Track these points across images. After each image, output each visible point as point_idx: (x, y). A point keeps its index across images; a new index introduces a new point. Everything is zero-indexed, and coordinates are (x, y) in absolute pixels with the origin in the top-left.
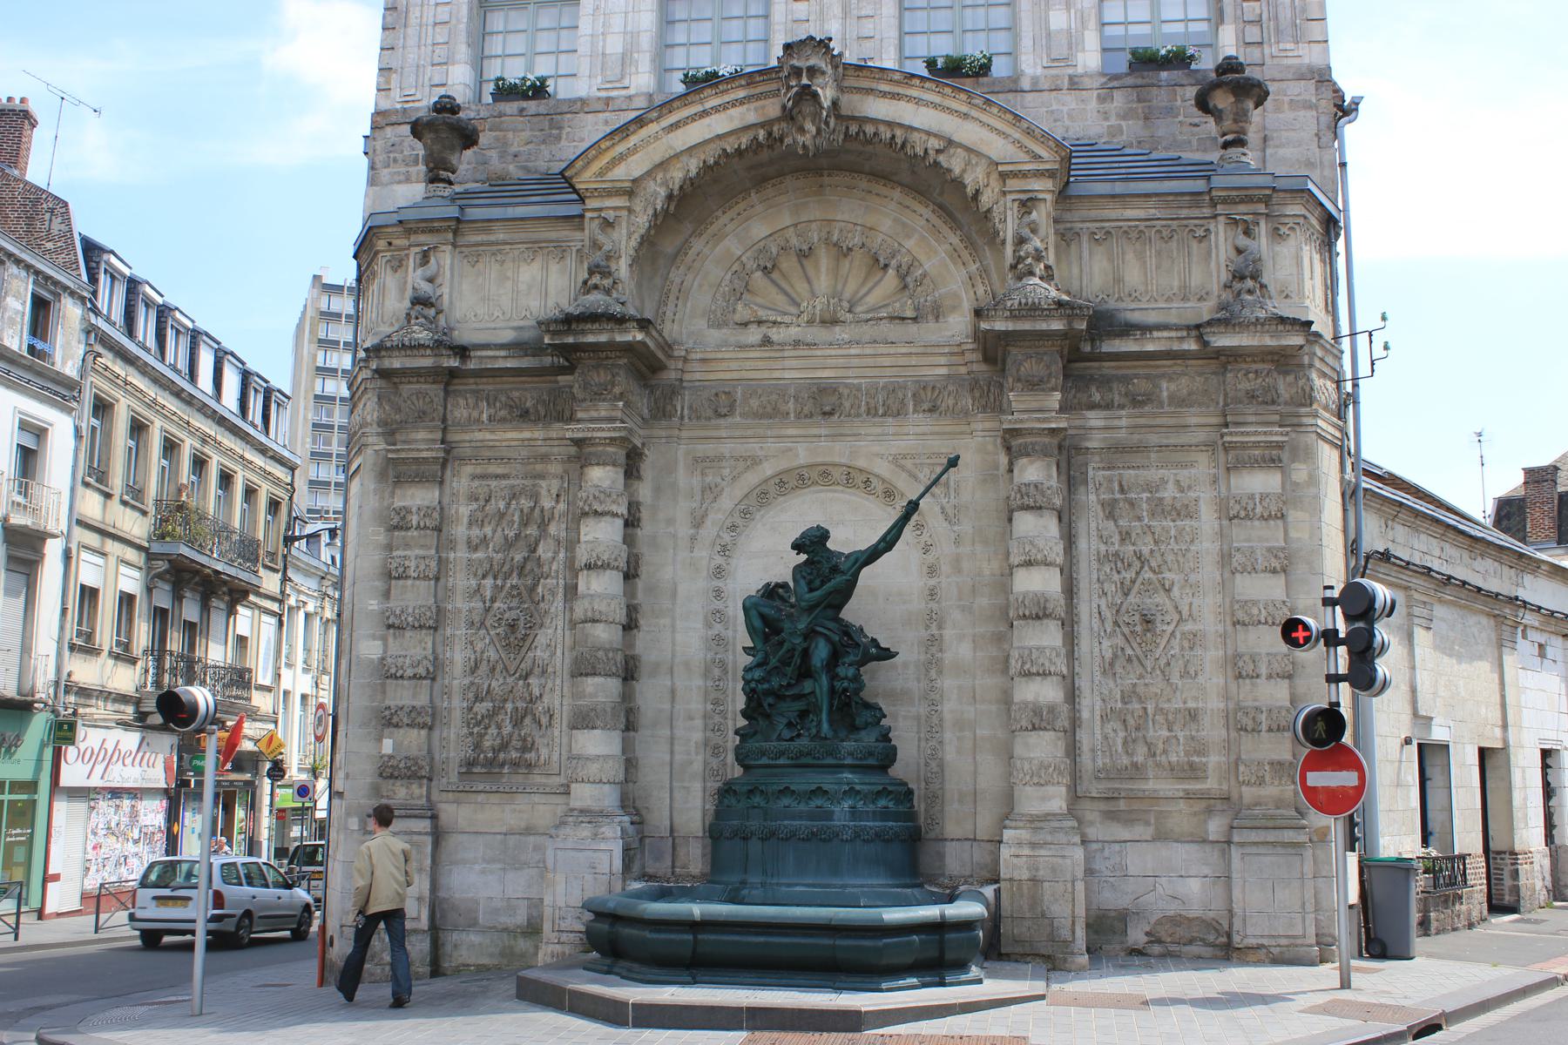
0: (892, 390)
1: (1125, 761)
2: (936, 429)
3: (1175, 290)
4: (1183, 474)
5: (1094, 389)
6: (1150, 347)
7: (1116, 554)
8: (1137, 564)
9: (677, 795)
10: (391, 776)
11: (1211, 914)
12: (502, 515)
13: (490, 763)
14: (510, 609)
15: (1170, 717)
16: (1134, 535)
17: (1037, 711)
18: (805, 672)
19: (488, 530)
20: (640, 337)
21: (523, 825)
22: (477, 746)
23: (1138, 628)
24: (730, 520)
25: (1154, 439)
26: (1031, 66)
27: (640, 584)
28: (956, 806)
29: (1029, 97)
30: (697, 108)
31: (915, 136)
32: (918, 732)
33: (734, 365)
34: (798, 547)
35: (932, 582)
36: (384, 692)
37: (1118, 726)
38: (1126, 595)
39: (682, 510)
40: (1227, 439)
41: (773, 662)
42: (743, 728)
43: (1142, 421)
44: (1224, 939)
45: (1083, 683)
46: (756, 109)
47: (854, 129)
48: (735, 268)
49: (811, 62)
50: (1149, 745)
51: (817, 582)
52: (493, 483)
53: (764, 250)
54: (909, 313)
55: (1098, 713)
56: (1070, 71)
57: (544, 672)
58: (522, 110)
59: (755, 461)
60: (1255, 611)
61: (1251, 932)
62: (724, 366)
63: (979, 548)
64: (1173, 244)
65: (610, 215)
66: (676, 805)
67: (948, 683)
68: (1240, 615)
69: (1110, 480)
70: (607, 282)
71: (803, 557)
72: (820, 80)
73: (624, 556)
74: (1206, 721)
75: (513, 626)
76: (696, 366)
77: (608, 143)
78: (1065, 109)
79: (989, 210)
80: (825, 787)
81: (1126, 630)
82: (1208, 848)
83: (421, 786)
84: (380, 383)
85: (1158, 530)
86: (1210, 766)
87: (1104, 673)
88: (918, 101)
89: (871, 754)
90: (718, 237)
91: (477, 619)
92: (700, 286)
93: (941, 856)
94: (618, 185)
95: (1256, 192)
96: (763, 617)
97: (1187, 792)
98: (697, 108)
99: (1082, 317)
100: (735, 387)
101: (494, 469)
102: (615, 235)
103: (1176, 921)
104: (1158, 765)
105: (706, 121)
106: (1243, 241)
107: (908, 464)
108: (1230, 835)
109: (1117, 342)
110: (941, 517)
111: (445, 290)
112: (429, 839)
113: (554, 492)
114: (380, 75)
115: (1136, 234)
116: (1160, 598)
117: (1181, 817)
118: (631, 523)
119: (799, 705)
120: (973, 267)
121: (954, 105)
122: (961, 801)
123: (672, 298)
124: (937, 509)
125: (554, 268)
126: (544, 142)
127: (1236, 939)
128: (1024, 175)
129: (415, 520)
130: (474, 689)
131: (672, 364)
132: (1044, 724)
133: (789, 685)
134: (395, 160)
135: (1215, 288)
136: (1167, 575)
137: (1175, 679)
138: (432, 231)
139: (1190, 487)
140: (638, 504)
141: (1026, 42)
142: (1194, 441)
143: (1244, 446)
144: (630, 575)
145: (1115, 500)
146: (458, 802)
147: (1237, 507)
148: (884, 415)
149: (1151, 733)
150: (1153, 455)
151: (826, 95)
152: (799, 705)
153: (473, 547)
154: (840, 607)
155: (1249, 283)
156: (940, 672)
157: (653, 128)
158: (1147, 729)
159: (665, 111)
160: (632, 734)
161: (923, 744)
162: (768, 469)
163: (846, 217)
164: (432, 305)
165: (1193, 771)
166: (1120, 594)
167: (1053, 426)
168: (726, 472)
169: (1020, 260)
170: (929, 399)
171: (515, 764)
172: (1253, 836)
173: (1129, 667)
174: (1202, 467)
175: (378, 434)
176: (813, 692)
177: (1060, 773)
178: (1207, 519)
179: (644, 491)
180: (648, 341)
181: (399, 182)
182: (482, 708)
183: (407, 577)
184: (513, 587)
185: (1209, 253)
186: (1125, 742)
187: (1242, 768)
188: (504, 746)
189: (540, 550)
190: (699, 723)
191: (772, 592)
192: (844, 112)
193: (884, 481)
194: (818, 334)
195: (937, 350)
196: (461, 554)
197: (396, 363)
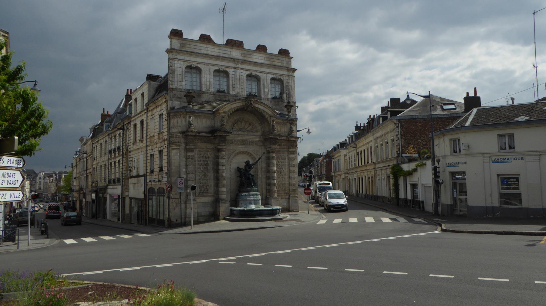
22: (201, 190)
26: (262, 96)
34: (245, 163)
61: (291, 210)
153: (198, 161)
182: (201, 185)
196: (197, 162)
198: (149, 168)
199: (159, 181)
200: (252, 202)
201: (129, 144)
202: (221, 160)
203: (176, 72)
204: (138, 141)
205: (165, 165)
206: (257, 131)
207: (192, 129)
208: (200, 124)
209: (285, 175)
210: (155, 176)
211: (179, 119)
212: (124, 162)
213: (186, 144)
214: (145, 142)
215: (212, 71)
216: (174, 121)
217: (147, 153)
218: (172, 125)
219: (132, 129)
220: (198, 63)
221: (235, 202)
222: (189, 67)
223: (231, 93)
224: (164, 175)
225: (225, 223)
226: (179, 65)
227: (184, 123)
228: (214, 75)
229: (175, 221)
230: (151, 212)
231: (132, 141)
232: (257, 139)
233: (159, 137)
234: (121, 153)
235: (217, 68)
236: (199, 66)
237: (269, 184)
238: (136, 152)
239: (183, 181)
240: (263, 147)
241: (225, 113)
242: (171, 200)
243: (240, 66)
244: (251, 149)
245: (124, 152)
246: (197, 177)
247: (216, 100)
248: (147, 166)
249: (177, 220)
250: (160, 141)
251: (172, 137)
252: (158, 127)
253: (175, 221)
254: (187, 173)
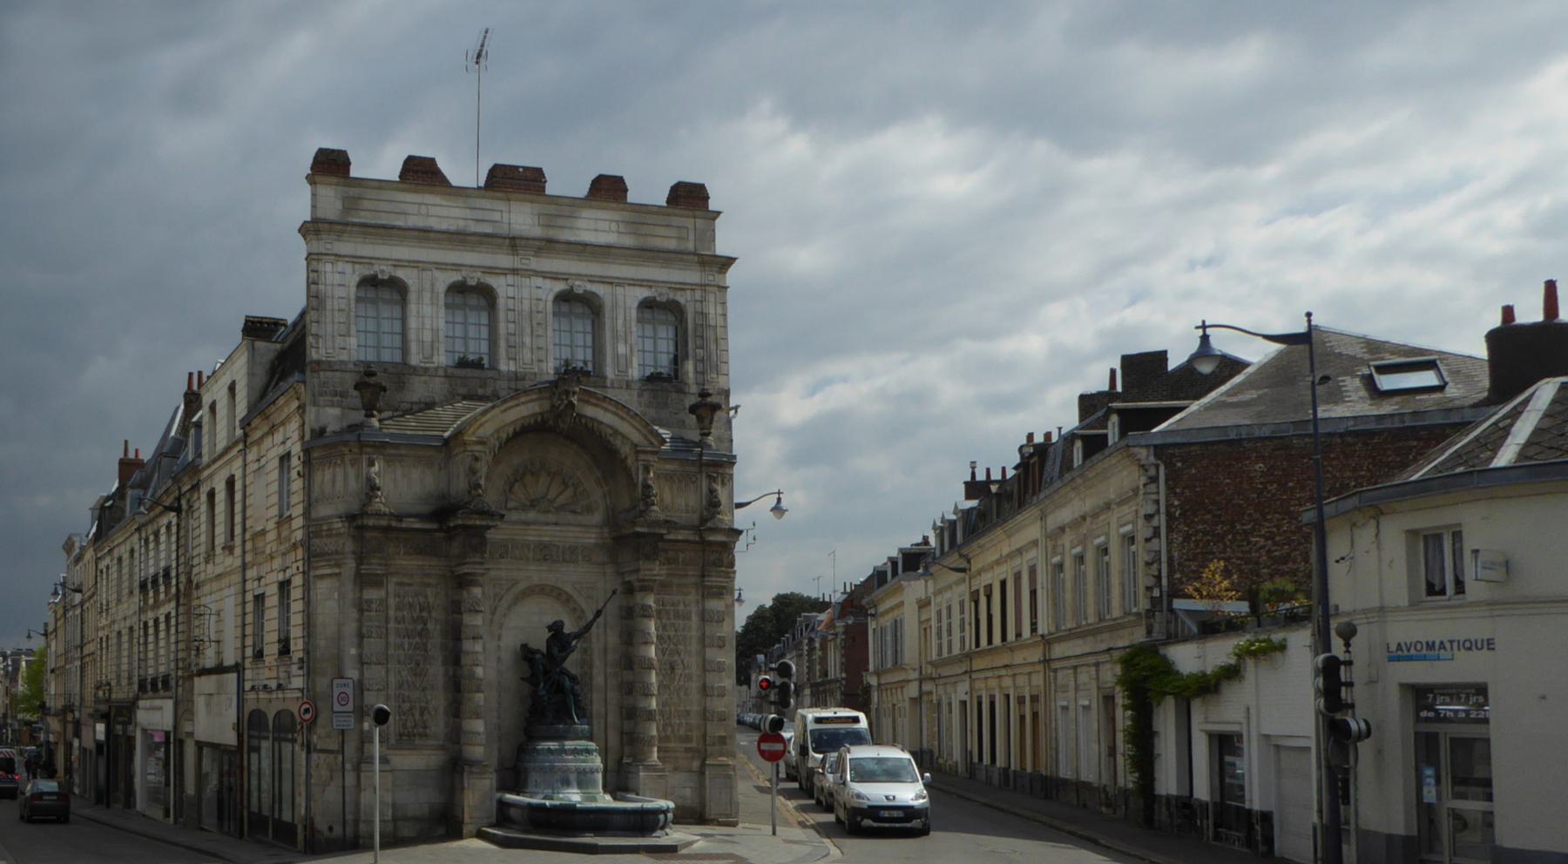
12: (411, 605)
101: (406, 580)
196: (392, 625)
198: (249, 641)
199: (280, 687)
200: (573, 777)
201: (196, 561)
202: (468, 619)
204: (218, 550)
205: (296, 632)
206: (589, 510)
207: (379, 504)
208: (402, 486)
209: (689, 678)
210: (267, 674)
211: (339, 471)
212: (181, 619)
213: (360, 559)
214: (238, 551)
215: (441, 288)
216: (324, 477)
217: (244, 592)
218: (316, 493)
219: (204, 508)
221: (514, 776)
222: (370, 282)
223: (503, 366)
224: (294, 669)
225: (482, 851)
227: (353, 484)
228: (447, 306)
229: (326, 833)
230: (255, 794)
231: (203, 549)
232: (590, 538)
233: (279, 535)
234: (173, 590)
235: (455, 277)
237: (631, 714)
238: (215, 585)
239: (350, 691)
240: (610, 569)
241: (481, 442)
242: (314, 756)
244: (570, 576)
245: (182, 587)
246: (392, 679)
247: (451, 398)
248: (244, 636)
249: (331, 829)
250: (283, 548)
251: (318, 534)
252: (275, 499)
253: (326, 833)
254: (362, 662)
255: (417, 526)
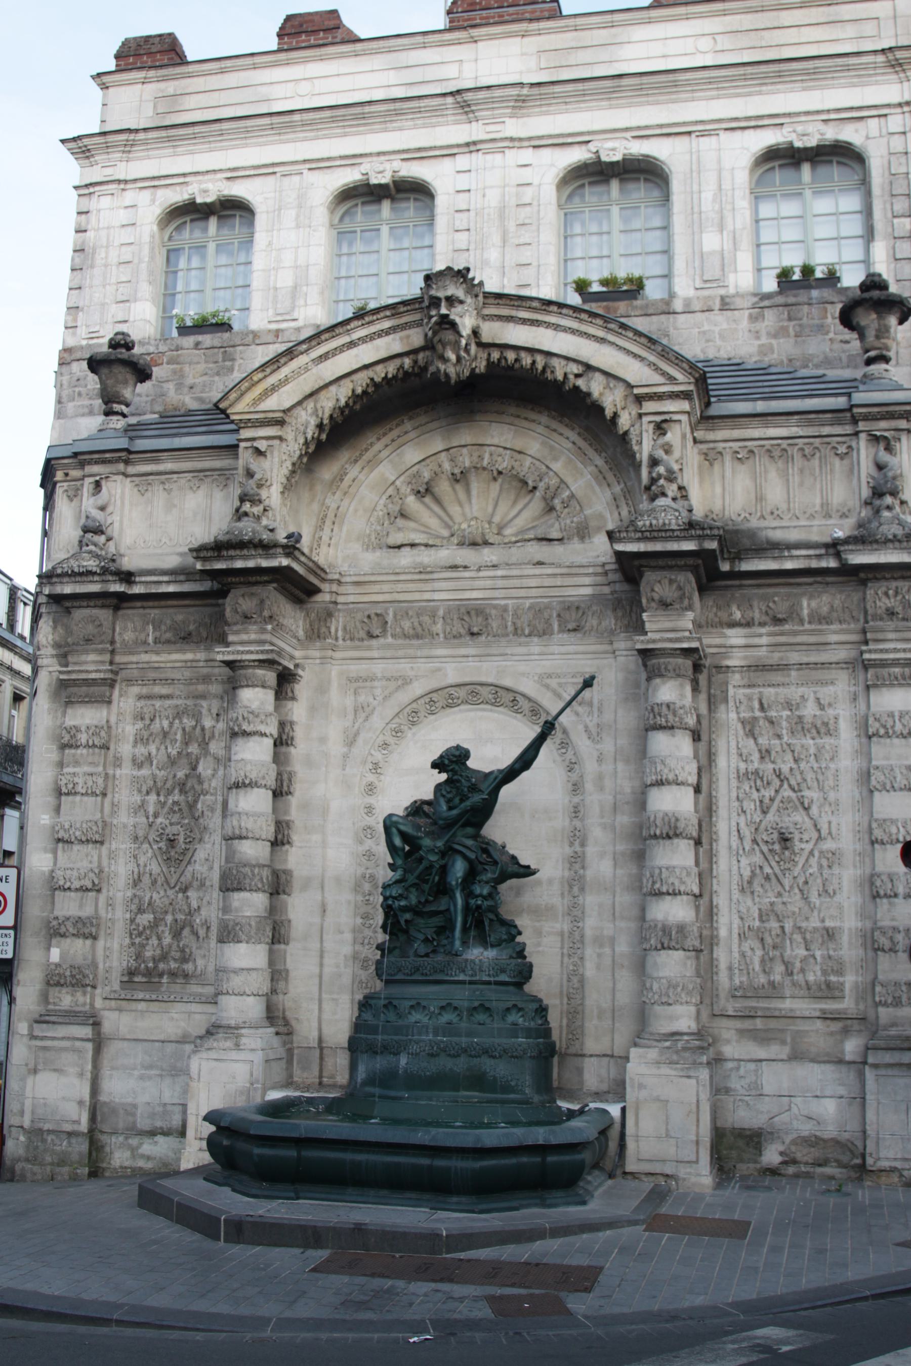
0: (538, 611)
1: (763, 979)
2: (581, 648)
3: (818, 508)
4: (826, 693)
5: (734, 608)
6: (789, 565)
7: (756, 773)
8: (777, 782)
9: (325, 1006)
10: (58, 984)
11: (846, 1136)
12: (165, 734)
13: (148, 973)
14: (171, 824)
15: (808, 936)
16: (773, 754)
17: (666, 930)
18: (443, 890)
19: (153, 748)
20: (285, 562)
21: (180, 1032)
22: (138, 956)
23: (777, 847)
24: (381, 738)
25: (795, 657)
26: (684, 288)
27: (294, 801)
28: (595, 1022)
29: (682, 318)
30: (345, 339)
31: (555, 362)
32: (562, 948)
33: (386, 587)
35: (576, 800)
36: (53, 903)
37: (756, 944)
38: (764, 812)
39: (334, 730)
40: (866, 656)
41: (411, 879)
42: (384, 943)
43: (782, 639)
44: (858, 1161)
45: (721, 901)
46: (401, 339)
47: (495, 355)
48: (390, 491)
49: (449, 293)
50: (786, 964)
51: (457, 800)
52: (158, 704)
53: (418, 475)
54: (555, 535)
55: (735, 931)
56: (722, 292)
57: (202, 885)
58: (197, 345)
59: (406, 681)
60: (894, 830)
62: (376, 588)
63: (620, 766)
64: (816, 462)
65: (262, 445)
66: (325, 1016)
67: (590, 900)
68: (878, 833)
69: (750, 699)
70: (257, 510)
71: (444, 777)
72: (459, 309)
73: (273, 775)
74: (845, 939)
75: (172, 842)
76: (350, 589)
77: (260, 375)
78: (717, 329)
79: (626, 433)
80: (455, 1003)
81: (765, 848)
82: (844, 1068)
83: (84, 994)
84: (54, 608)
85: (798, 749)
86: (848, 986)
87: (742, 890)
88: (557, 327)
89: (503, 971)
90: (373, 463)
91: (141, 833)
92: (356, 511)
93: (580, 1071)
94: (271, 415)
95: (897, 408)
96: (404, 836)
97: (823, 1011)
98: (345, 339)
99: (712, 537)
100: (387, 609)
101: (158, 690)
102: (266, 464)
103: (813, 1141)
104: (794, 984)
105: (354, 351)
106: (884, 456)
107: (553, 683)
108: (866, 1056)
109: (756, 561)
110: (584, 736)
111: (116, 518)
112: (89, 1046)
113: (214, 711)
114: (67, 314)
115: (778, 452)
116: (798, 816)
117: (818, 1035)
118: (282, 741)
119: (437, 921)
120: (617, 489)
121: (592, 330)
122: (600, 1017)
123: (328, 523)
124: (581, 727)
125: (218, 495)
126: (218, 374)
127: (870, 1161)
128: (659, 397)
129: (83, 738)
130: (136, 901)
131: (325, 587)
132: (673, 944)
133: (427, 901)
134: (80, 394)
135: (854, 503)
136: (806, 793)
137: (814, 899)
138: (104, 462)
139: (830, 705)
140: (292, 723)
141: (679, 265)
142: (834, 659)
143: (883, 664)
144: (279, 793)
145: (755, 719)
146: (120, 1010)
147: (877, 725)
148: (530, 635)
149: (789, 951)
150: (793, 673)
151: (466, 322)
152: (437, 921)
153: (137, 764)
154: (480, 825)
155: (888, 500)
156: (582, 889)
157: (302, 360)
158: (783, 948)
159: (314, 343)
160: (282, 946)
161: (566, 959)
162: (418, 688)
163: (496, 441)
164: (102, 533)
165: (830, 991)
166: (759, 812)
167: (685, 645)
168: (378, 692)
169: (653, 481)
170: (572, 619)
171: (173, 974)
172: (889, 1058)
173: (767, 886)
174: (841, 686)
175: (53, 656)
176: (448, 910)
177: (689, 993)
178: (846, 736)
179: (298, 711)
180: (296, 566)
181: (83, 415)
182: (145, 919)
183: (76, 793)
184: (175, 803)
185: (851, 470)
186: (763, 961)
187: (878, 989)
188: (164, 957)
189: (200, 768)
190: (348, 936)
191: (417, 809)
192: (486, 338)
193: (530, 699)
194: (466, 556)
195: (582, 571)
197: (68, 589)
203: (101, 255)
220: (234, 174)
226: (123, 216)
236: (238, 190)
243: (513, 127)
255: (171, 589)
